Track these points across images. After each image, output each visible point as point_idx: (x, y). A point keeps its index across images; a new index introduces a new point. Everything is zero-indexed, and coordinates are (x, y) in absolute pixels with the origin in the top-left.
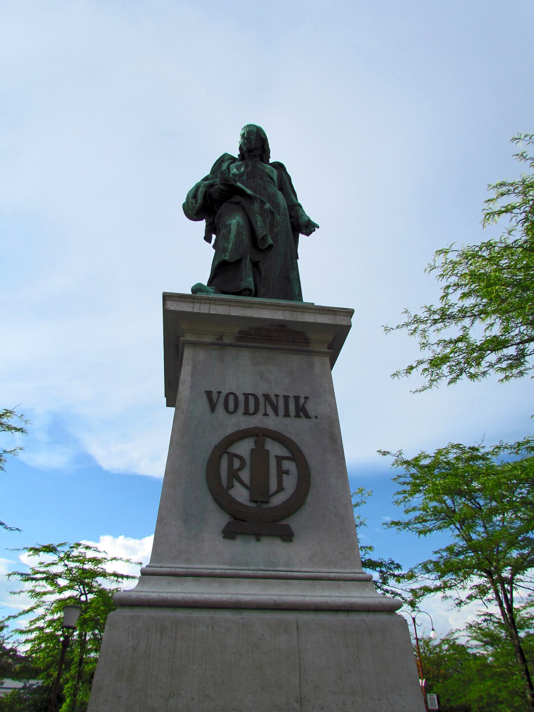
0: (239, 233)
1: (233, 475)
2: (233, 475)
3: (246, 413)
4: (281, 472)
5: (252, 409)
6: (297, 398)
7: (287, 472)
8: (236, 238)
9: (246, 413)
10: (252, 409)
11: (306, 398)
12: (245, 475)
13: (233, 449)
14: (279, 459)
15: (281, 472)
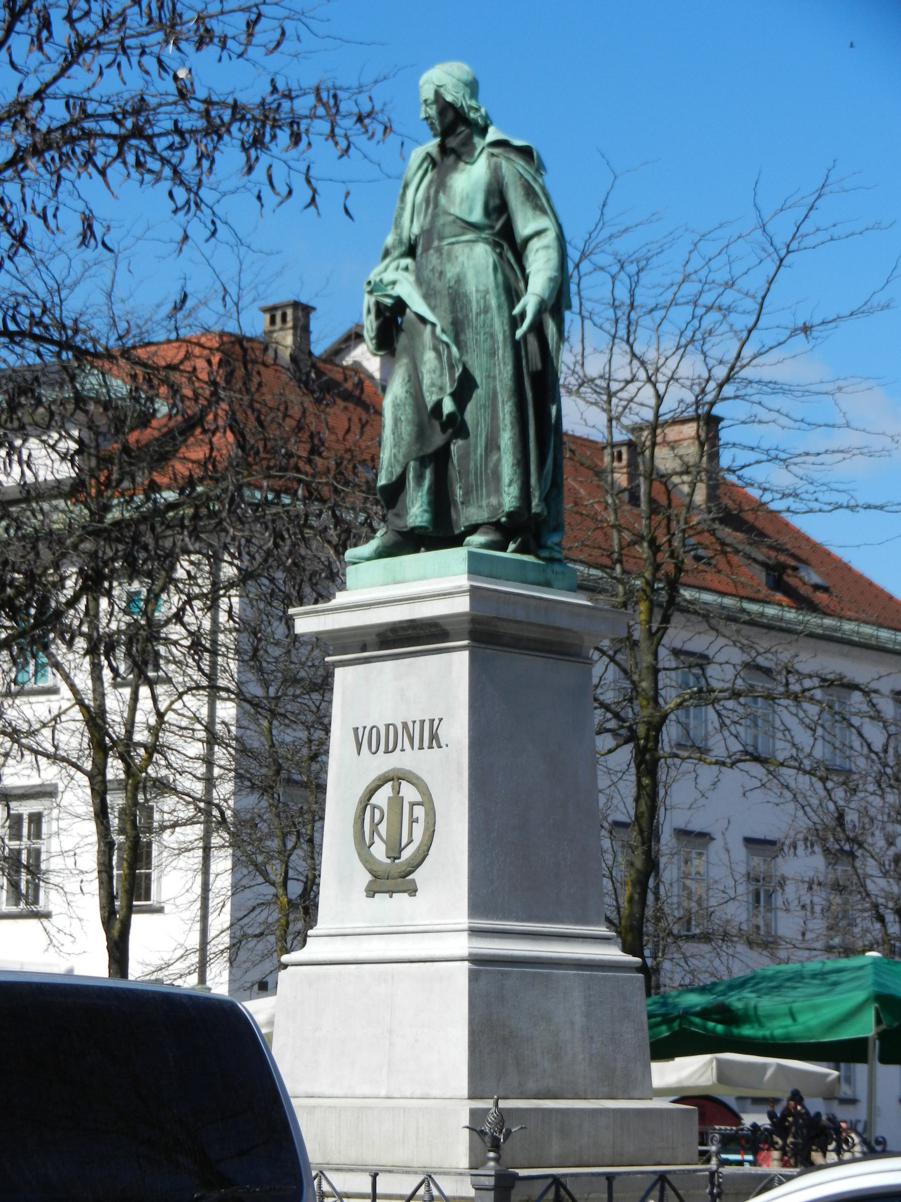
0: (396, 421)
1: (374, 829)
2: (374, 829)
3: (387, 752)
4: (413, 821)
5: (391, 748)
6: (432, 721)
7: (417, 821)
8: (394, 434)
9: (387, 752)
10: (391, 748)
11: (441, 720)
12: (383, 828)
13: (374, 800)
14: (412, 805)
15: (413, 821)
